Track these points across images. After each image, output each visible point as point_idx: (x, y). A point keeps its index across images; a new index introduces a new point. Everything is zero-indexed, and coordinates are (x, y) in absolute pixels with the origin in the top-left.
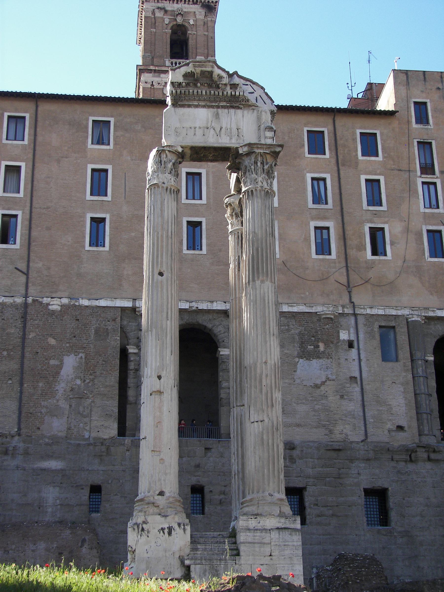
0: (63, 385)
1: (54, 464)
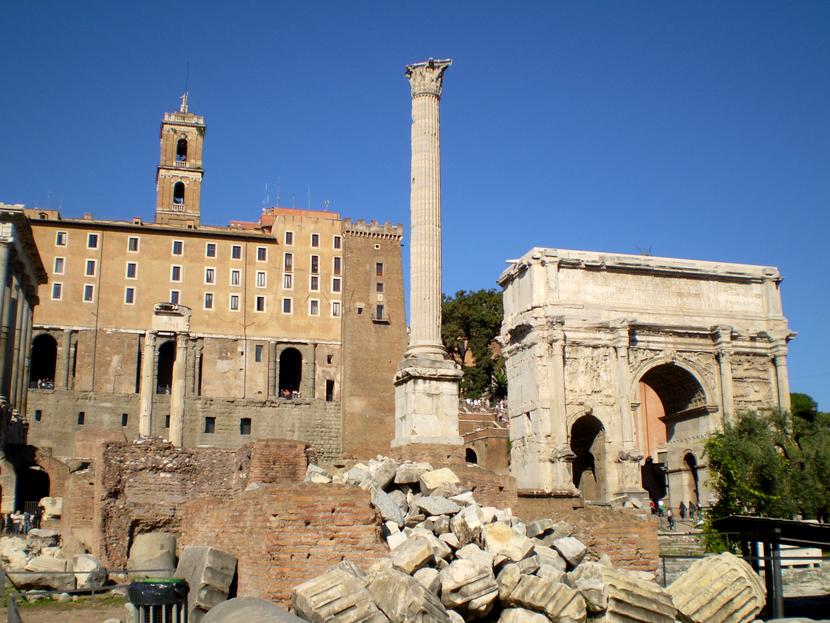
1: (108, 405)
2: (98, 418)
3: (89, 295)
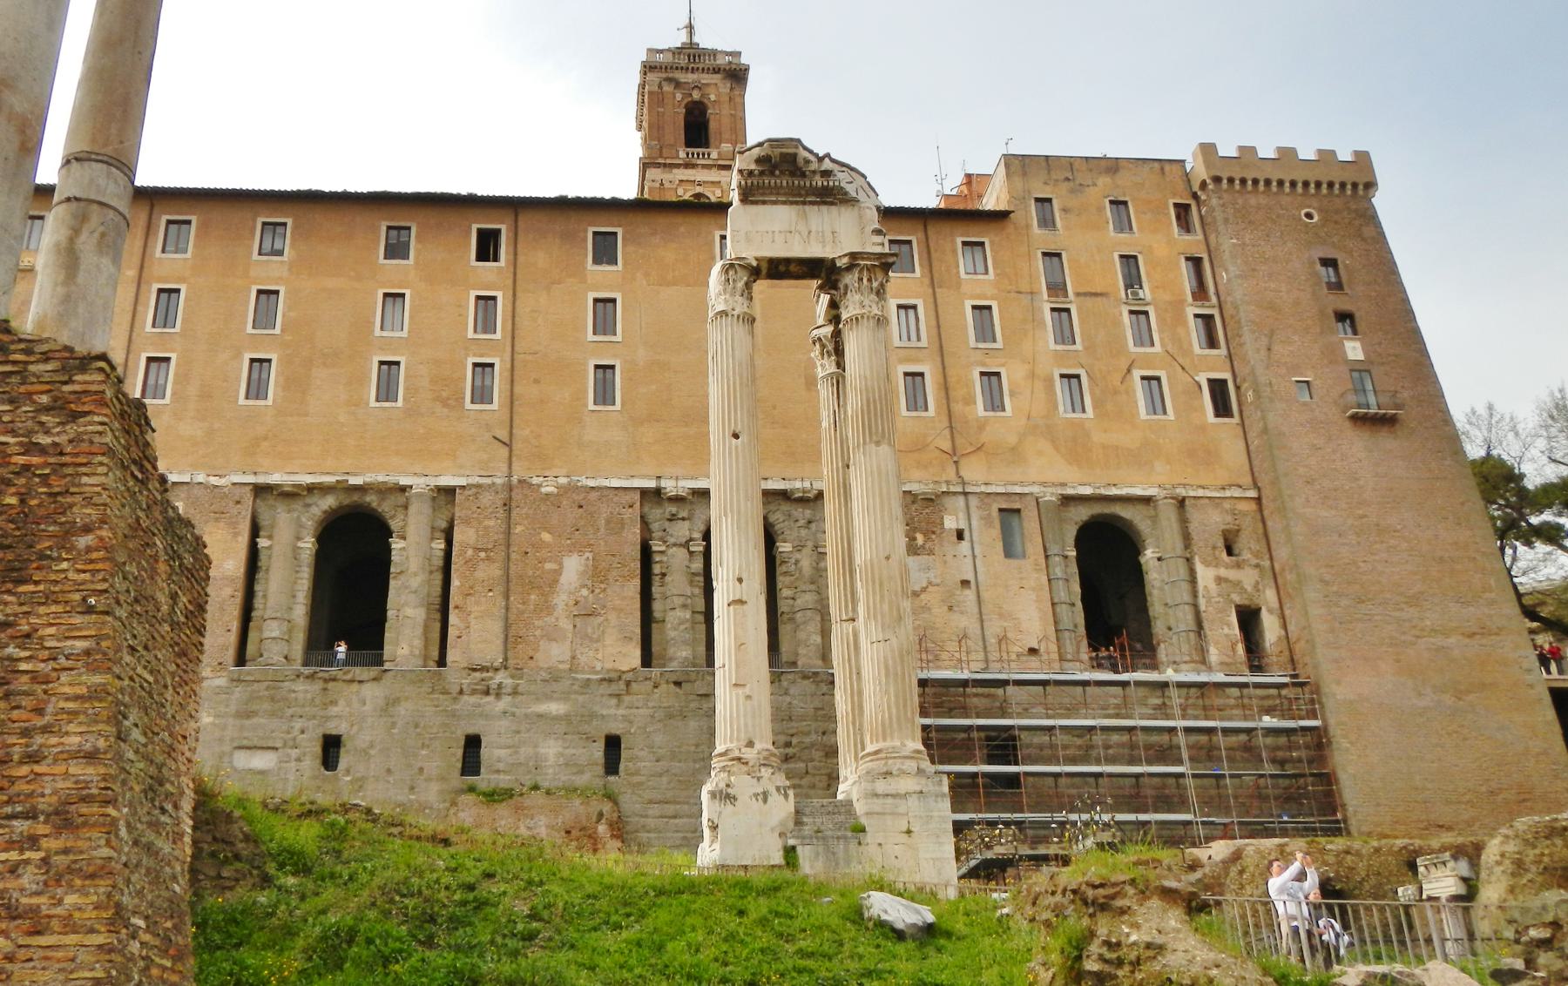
0: (564, 597)
1: (555, 708)
2: (525, 751)
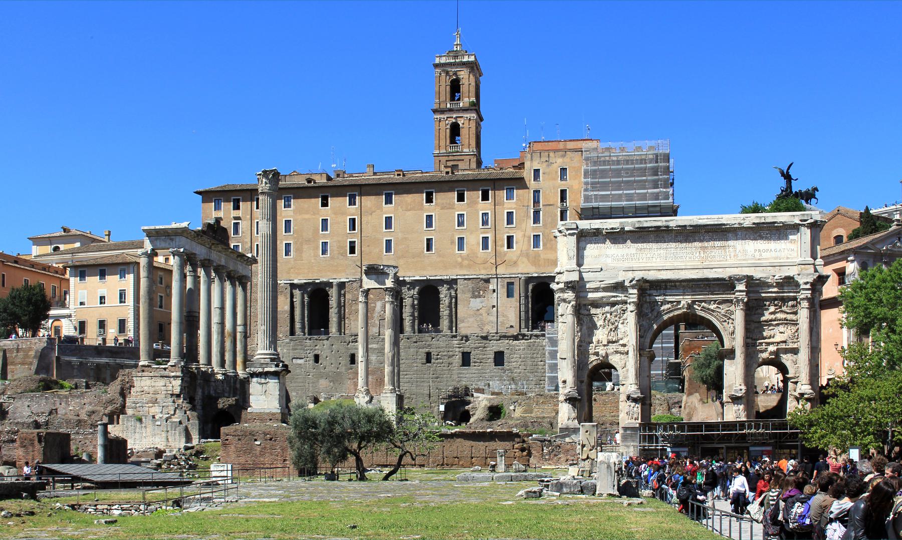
3: (352, 251)
